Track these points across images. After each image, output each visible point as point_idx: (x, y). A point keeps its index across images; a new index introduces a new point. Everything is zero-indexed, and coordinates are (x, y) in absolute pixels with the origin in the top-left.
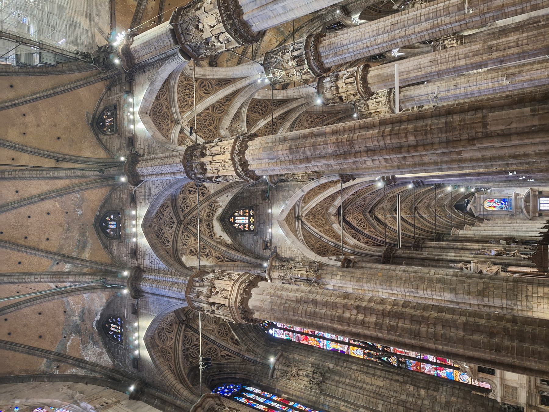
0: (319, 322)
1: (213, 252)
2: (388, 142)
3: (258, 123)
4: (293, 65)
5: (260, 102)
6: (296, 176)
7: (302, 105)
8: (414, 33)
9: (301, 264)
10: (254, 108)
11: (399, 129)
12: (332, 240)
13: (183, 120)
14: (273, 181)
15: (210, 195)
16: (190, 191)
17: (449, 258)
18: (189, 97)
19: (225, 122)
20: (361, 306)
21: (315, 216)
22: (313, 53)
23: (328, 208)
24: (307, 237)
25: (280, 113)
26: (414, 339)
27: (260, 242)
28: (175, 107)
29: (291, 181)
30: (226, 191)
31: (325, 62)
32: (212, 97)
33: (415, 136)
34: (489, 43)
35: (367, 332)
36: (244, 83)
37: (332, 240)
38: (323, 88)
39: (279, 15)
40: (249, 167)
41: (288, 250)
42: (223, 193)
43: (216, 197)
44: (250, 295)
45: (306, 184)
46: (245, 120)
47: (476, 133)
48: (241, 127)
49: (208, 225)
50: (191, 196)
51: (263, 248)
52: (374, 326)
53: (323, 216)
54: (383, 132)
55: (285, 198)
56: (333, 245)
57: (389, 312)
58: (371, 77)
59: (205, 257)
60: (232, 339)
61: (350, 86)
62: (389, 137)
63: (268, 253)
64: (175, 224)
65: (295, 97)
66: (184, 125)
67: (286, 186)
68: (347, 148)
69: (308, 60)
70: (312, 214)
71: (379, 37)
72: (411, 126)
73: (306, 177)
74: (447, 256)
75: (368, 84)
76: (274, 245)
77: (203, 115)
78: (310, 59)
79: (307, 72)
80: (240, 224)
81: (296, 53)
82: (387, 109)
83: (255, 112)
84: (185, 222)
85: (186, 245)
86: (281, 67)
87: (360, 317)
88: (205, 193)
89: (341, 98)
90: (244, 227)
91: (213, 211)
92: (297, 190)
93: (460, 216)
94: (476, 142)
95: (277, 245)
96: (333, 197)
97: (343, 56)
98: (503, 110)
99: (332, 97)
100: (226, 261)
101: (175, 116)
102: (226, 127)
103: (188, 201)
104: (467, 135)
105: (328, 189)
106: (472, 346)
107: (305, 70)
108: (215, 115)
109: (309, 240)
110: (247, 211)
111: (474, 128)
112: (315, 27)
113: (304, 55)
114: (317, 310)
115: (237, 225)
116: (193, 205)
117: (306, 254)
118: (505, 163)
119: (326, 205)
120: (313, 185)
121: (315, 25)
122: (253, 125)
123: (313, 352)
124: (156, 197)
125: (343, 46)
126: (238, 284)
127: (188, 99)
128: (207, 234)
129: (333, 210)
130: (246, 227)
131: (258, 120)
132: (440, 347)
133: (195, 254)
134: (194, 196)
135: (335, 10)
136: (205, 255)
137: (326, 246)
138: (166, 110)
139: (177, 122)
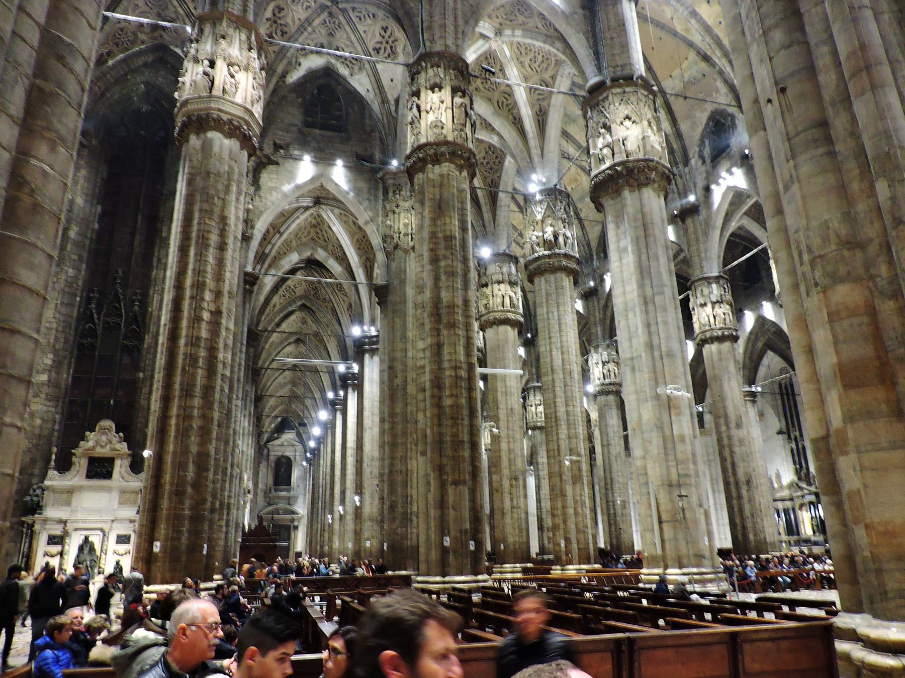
0: (192, 252)
2: (448, 373)
6: (391, 216)
7: (484, 226)
8: (555, 397)
11: (461, 387)
12: (274, 251)
13: (500, 42)
14: (387, 177)
16: (385, 29)
20: (221, 317)
21: (315, 227)
22: (557, 264)
23: (325, 249)
26: (182, 390)
27: (288, 138)
28: (523, 36)
29: (384, 207)
30: (377, 91)
31: (543, 279)
33: (451, 406)
34: (521, 477)
35: (184, 323)
36: (535, 152)
37: (274, 251)
38: (503, 262)
39: (618, 241)
41: (273, 185)
42: (375, 86)
43: (370, 72)
44: (229, 135)
50: (377, 29)
51: (278, 142)
52: (195, 335)
53: (313, 239)
55: (358, 191)
57: (216, 358)
58: (507, 331)
59: (268, 32)
60: (109, 54)
61: (499, 300)
62: (453, 374)
65: (497, 217)
67: (376, 196)
68: (445, 319)
69: (549, 256)
70: (318, 224)
72: (463, 401)
73: (388, 233)
76: (280, 160)
79: (534, 251)
81: (561, 239)
83: (487, 153)
84: (334, 9)
86: (547, 213)
87: (206, 315)
88: (378, 53)
89: (486, 285)
92: (370, 213)
93: (270, 424)
94: (437, 473)
96: (343, 259)
97: (545, 304)
98: (470, 501)
101: (508, 32)
103: (369, 21)
106: (180, 462)
107: (537, 249)
111: (454, 471)
113: (557, 251)
114: (211, 250)
116: (361, 28)
118: (385, 496)
119: (330, 247)
120: (376, 241)
123: (92, 204)
125: (558, 307)
126: (247, 117)
127: (529, 57)
129: (321, 255)
132: (173, 421)
134: (377, 34)
135: (594, 280)
139: (498, 33)
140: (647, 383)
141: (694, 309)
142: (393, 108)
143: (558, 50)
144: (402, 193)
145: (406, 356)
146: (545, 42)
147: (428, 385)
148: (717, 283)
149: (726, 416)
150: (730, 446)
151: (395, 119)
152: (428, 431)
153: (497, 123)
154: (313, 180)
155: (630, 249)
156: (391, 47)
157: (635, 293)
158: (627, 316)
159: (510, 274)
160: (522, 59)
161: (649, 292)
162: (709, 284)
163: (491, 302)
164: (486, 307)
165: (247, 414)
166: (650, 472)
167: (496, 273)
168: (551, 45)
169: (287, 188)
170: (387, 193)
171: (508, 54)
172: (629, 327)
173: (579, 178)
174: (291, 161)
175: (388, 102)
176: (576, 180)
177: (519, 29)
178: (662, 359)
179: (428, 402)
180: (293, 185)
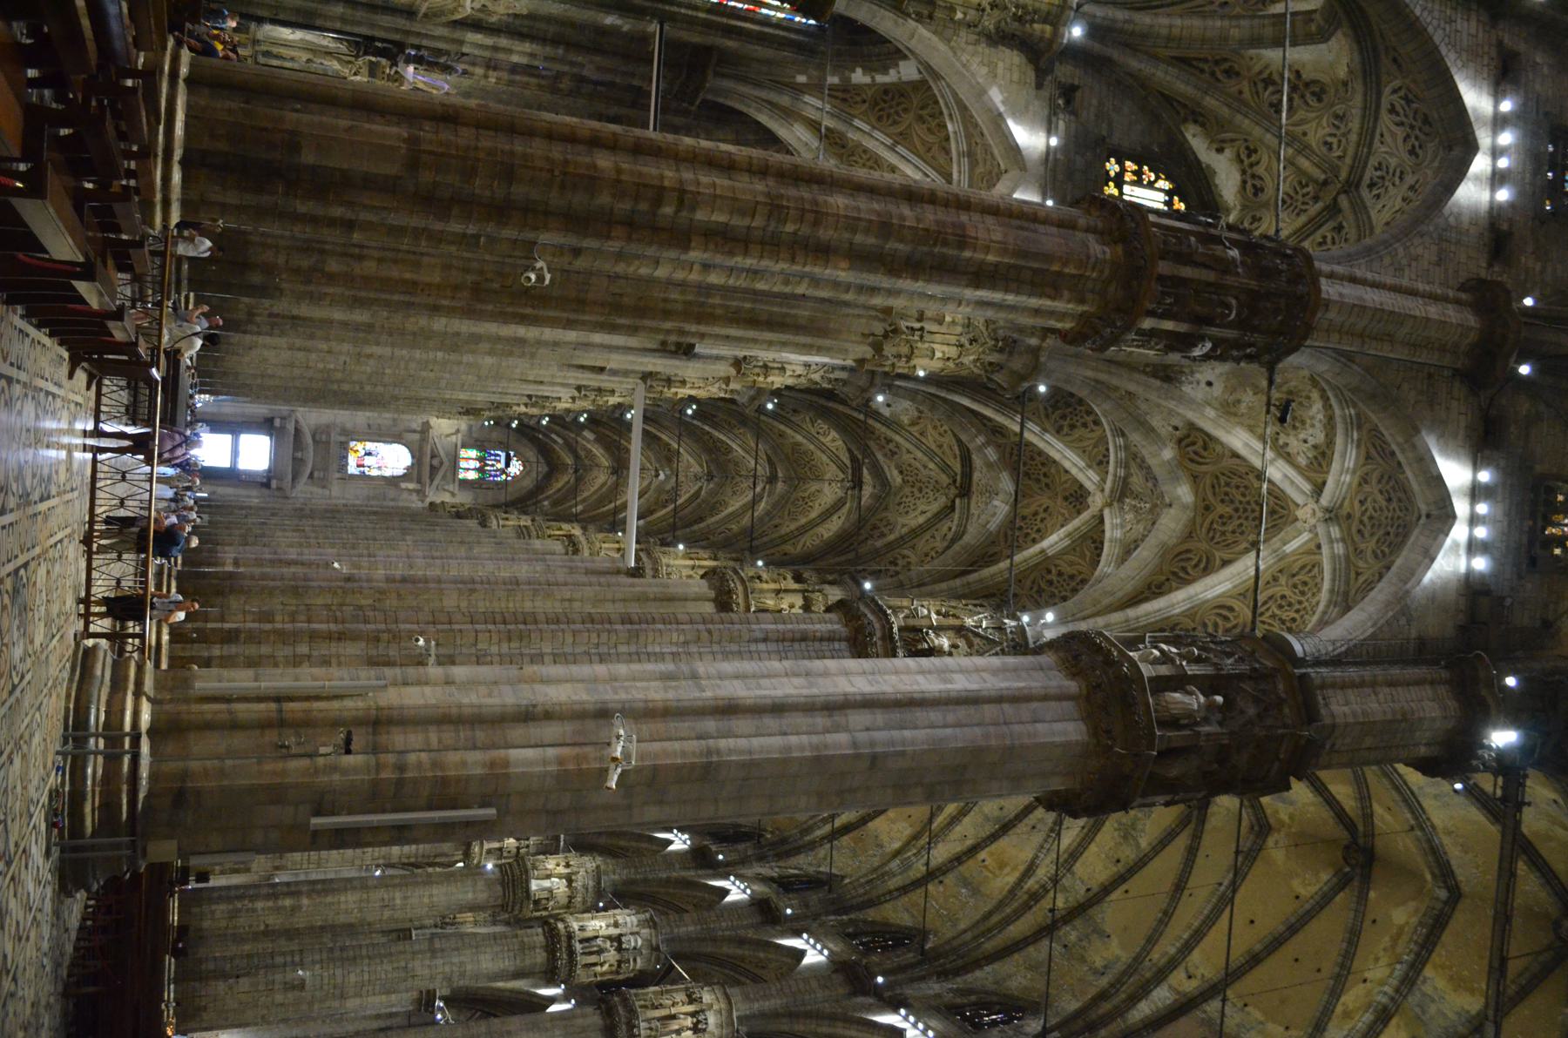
1: (1247, 95)
2: (669, 174)
3: (1067, 542)
4: (938, 635)
9: (959, 15)
13: (1313, 521)
17: (527, 47)
18: (1283, 597)
19: (1172, 525)
24: (935, 148)
25: (993, 569)
28: (1333, 557)
32: (1210, 595)
41: (1000, 71)
46: (1106, 545)
48: (1122, 526)
49: (1258, 190)
51: (1078, 94)
54: (681, 202)
56: (857, 122)
59: (1276, 77)
62: (666, 183)
63: (1065, 72)
64: (1366, 180)
66: (1312, 505)
71: (674, 649)
72: (604, 199)
74: (533, 55)
75: (715, 600)
76: (1045, 93)
77: (1245, 545)
78: (883, 638)
79: (896, 610)
80: (1151, 185)
82: (665, 560)
83: (1072, 577)
85: (1337, 117)
90: (1139, 173)
95: (1033, 92)
99: (826, 587)
100: (1206, 60)
102: (1172, 511)
108: (1204, 546)
109: (930, 138)
112: (862, 885)
115: (1163, 184)
117: (942, 47)
121: (861, 891)
122: (1084, 537)
124: (1423, 228)
127: (1287, 593)
128: (1265, 159)
130: (1134, 173)
131: (1064, 552)
133: (1307, 85)
136: (1274, 83)
137: (880, 119)
139: (1332, 515)
153: (1146, 554)
154: (1014, 150)
160: (1283, 580)
163: (765, 586)
165: (536, 63)
168: (1330, 602)
169: (996, 96)
171: (1289, 548)
172: (768, 676)
173: (1007, 870)
174: (1046, 112)
176: (1002, 865)
178: (699, 738)
180: (1002, 109)
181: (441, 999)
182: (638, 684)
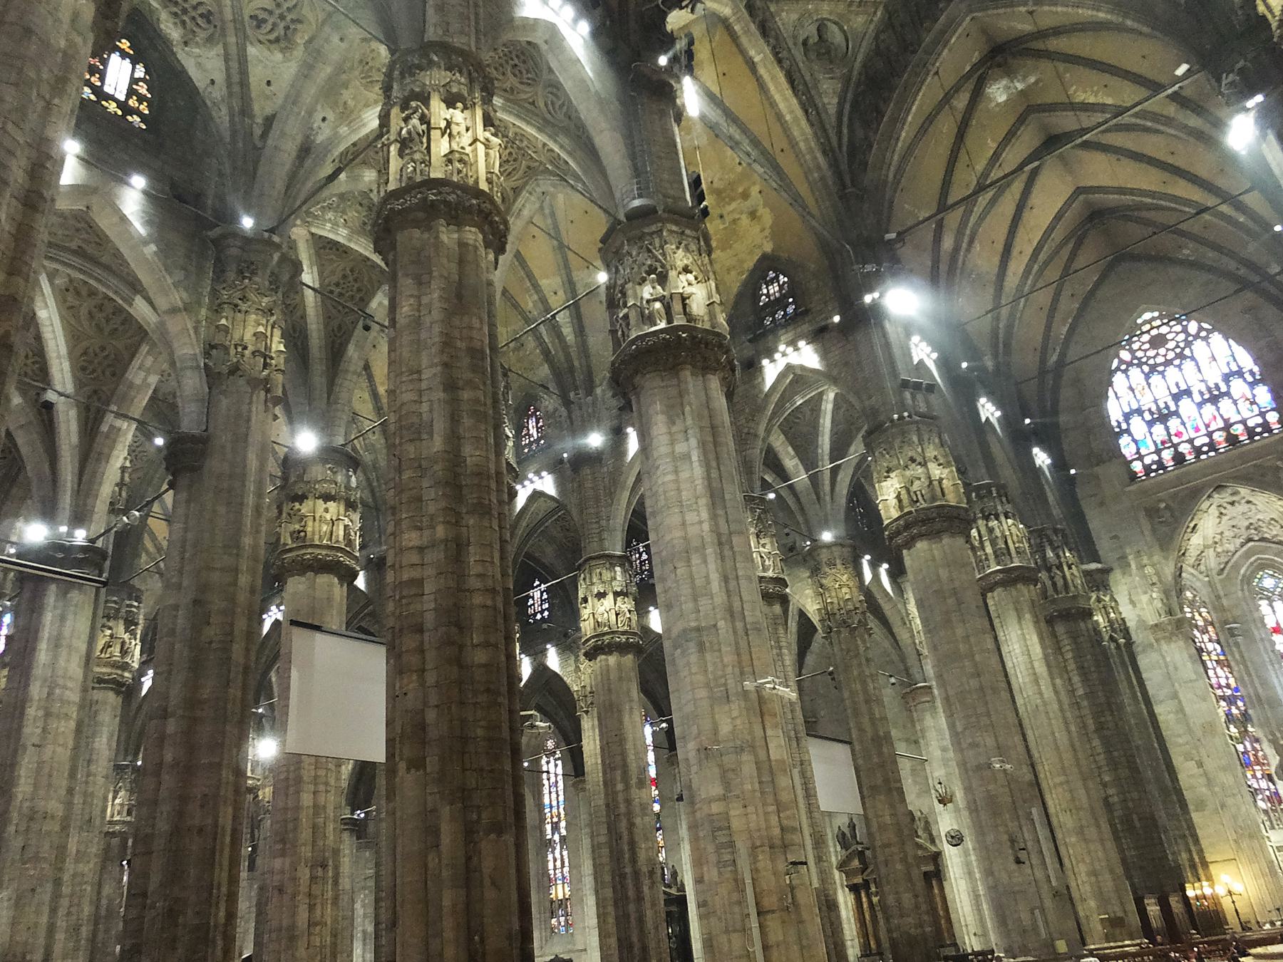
2: (478, 600)
3: (315, 269)
5: (362, 299)
6: (227, 311)
10: (355, 280)
14: (231, 241)
15: (246, 37)
29: (214, 293)
40: (442, 221)
42: (236, 78)
43: (233, 50)
45: (196, 329)
46: (352, 245)
47: (479, 807)
58: (331, 585)
67: (200, 269)
68: (471, 498)
83: (344, 277)
88: (259, 27)
89: (301, 498)
91: (185, 11)
92: (185, 295)
104: (474, 785)
105: (74, 376)
110: (144, 108)
122: (318, 254)
138: (508, 85)
140: (729, 670)
141: (585, 600)
142: (258, 131)
143: (562, 147)
144: (256, 279)
145: (235, 583)
146: (540, 130)
147: (429, 619)
148: (622, 566)
149: (625, 766)
150: (629, 814)
151: (258, 150)
152: (431, 716)
155: (695, 458)
156: (287, 28)
157: (706, 527)
158: (689, 560)
159: (348, 487)
161: (724, 528)
162: (612, 566)
164: (296, 535)
166: (736, 824)
167: (324, 481)
168: (550, 136)
170: (223, 271)
175: (252, 117)
177: (501, 96)
179: (431, 656)
181: (352, 814)
182: (710, 669)
